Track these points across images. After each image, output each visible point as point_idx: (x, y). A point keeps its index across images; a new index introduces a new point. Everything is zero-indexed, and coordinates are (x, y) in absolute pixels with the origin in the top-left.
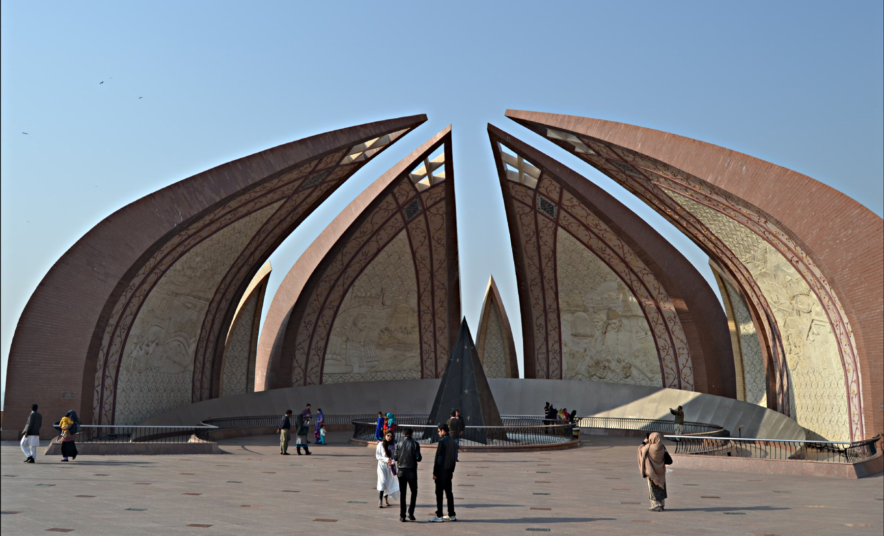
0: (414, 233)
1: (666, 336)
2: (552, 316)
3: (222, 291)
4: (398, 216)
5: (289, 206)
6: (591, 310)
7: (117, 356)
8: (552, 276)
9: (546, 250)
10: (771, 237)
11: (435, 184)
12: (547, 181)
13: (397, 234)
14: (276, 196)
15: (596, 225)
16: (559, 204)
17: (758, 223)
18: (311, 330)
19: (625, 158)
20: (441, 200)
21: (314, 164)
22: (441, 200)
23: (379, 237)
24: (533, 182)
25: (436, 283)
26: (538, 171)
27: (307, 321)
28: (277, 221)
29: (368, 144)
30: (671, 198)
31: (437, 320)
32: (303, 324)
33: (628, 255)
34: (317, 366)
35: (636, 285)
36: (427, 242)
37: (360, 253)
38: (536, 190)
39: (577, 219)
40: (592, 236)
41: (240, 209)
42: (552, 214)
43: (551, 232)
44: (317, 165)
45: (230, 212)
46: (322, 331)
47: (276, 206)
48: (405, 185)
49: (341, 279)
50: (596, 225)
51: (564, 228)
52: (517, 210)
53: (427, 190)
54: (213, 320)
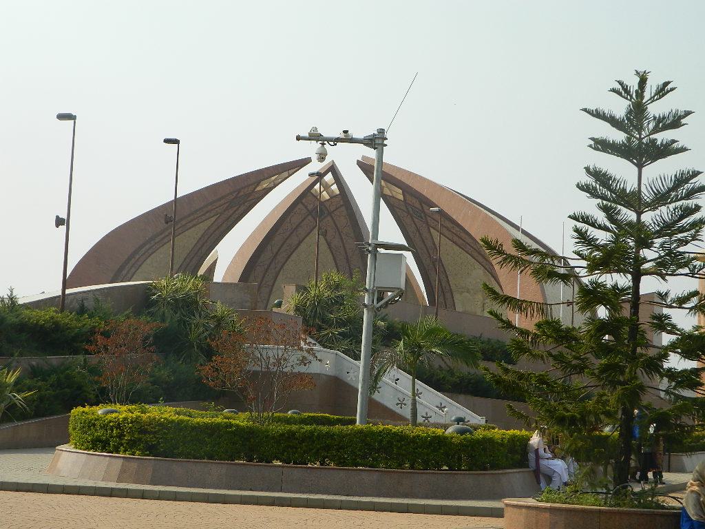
2: (448, 295)
4: (310, 217)
6: (472, 292)
9: (429, 244)
11: (333, 197)
14: (212, 215)
16: (423, 212)
20: (342, 206)
21: (234, 195)
22: (342, 206)
24: (401, 197)
26: (400, 191)
29: (273, 178)
37: (285, 245)
44: (238, 194)
47: (213, 219)
52: (399, 214)
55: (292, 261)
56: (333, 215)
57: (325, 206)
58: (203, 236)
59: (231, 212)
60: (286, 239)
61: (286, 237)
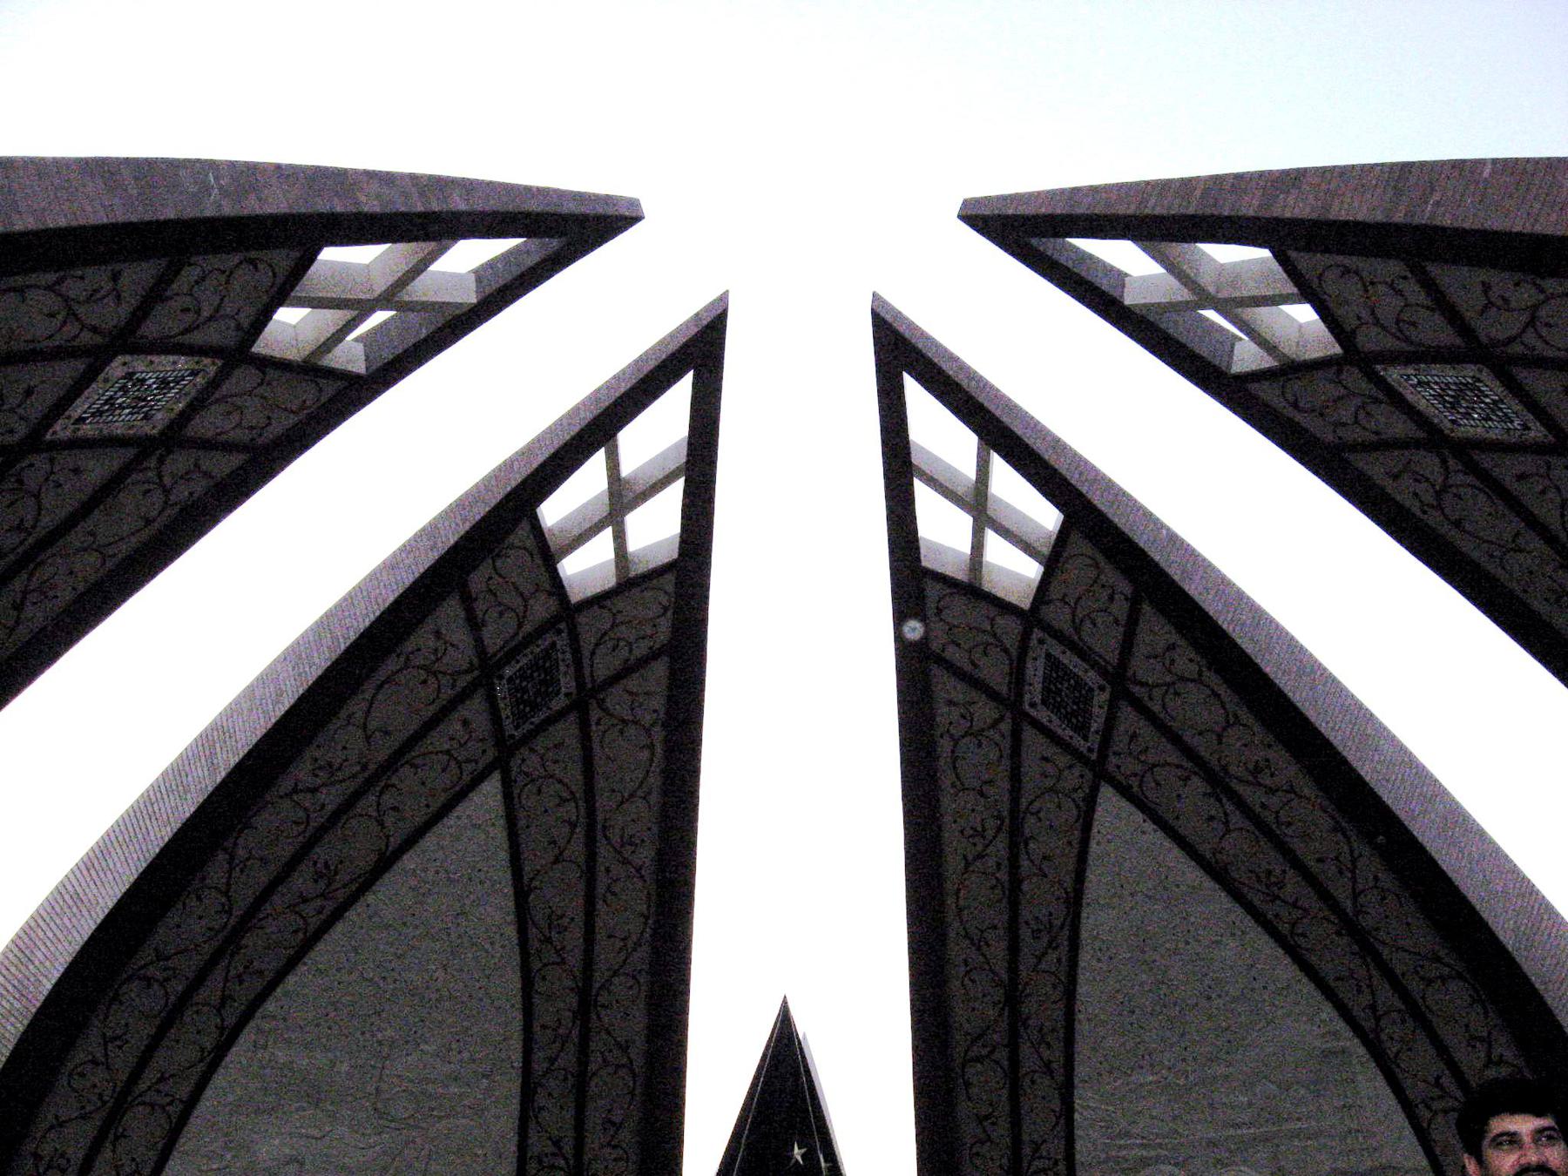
0: (529, 800)
4: (475, 708)
9: (1041, 901)
12: (1077, 571)
13: (461, 795)
15: (1257, 770)
16: (1119, 678)
20: (654, 655)
22: (654, 655)
23: (388, 799)
33: (1371, 898)
35: (1394, 1031)
36: (577, 850)
38: (1032, 617)
39: (1175, 739)
40: (1237, 819)
42: (1082, 729)
43: (1070, 812)
48: (515, 563)
49: (218, 974)
50: (1257, 770)
51: (1124, 791)
52: (945, 715)
53: (600, 600)
56: (595, 713)
60: (323, 829)
61: (317, 820)
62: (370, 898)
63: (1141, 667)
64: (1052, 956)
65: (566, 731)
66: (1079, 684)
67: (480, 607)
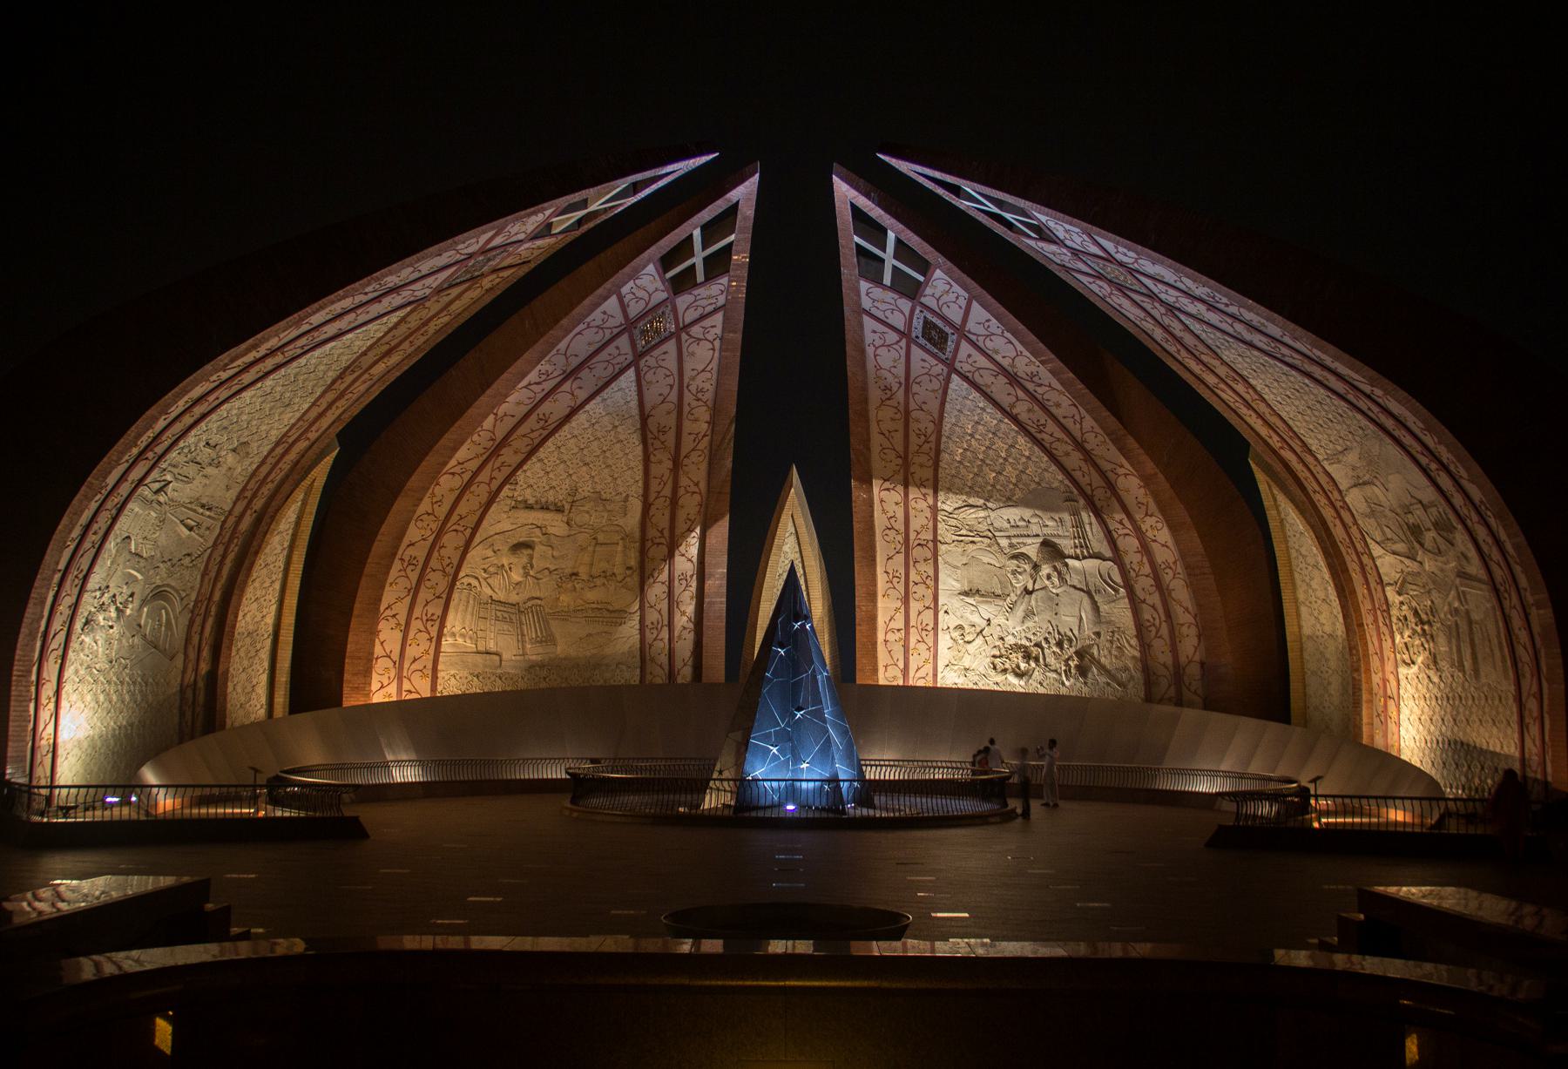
0: (649, 377)
1: (1155, 599)
3: (248, 494)
4: (624, 341)
5: (414, 321)
7: (61, 637)
8: (928, 473)
10: (1389, 423)
14: (397, 300)
15: (1033, 375)
16: (961, 331)
17: (1369, 397)
18: (414, 576)
19: (1119, 257)
20: (715, 311)
22: (715, 311)
25: (684, 481)
27: (407, 558)
28: (385, 348)
30: (1198, 337)
31: (678, 559)
32: (397, 565)
33: (1090, 437)
34: (427, 652)
37: (534, 417)
41: (325, 329)
42: (942, 350)
43: (936, 385)
45: (308, 332)
46: (437, 580)
47: (394, 318)
49: (489, 466)
51: (965, 378)
52: (869, 337)
54: (224, 557)
55: (541, 460)
57: (675, 310)
58: (341, 377)
59: (447, 299)
61: (540, 396)
62: (566, 427)
63: (971, 325)
64: (926, 446)
65: (671, 346)
66: (942, 331)
67: (626, 300)
